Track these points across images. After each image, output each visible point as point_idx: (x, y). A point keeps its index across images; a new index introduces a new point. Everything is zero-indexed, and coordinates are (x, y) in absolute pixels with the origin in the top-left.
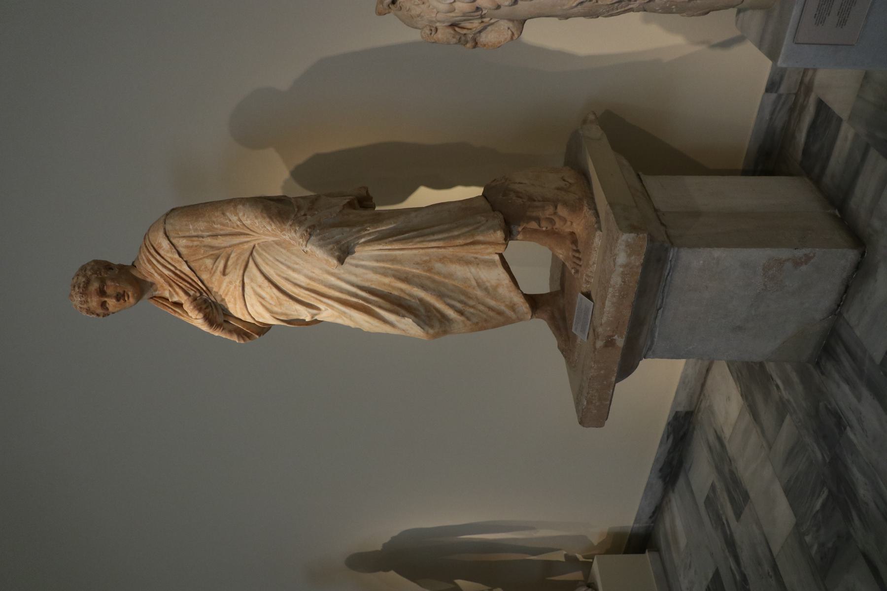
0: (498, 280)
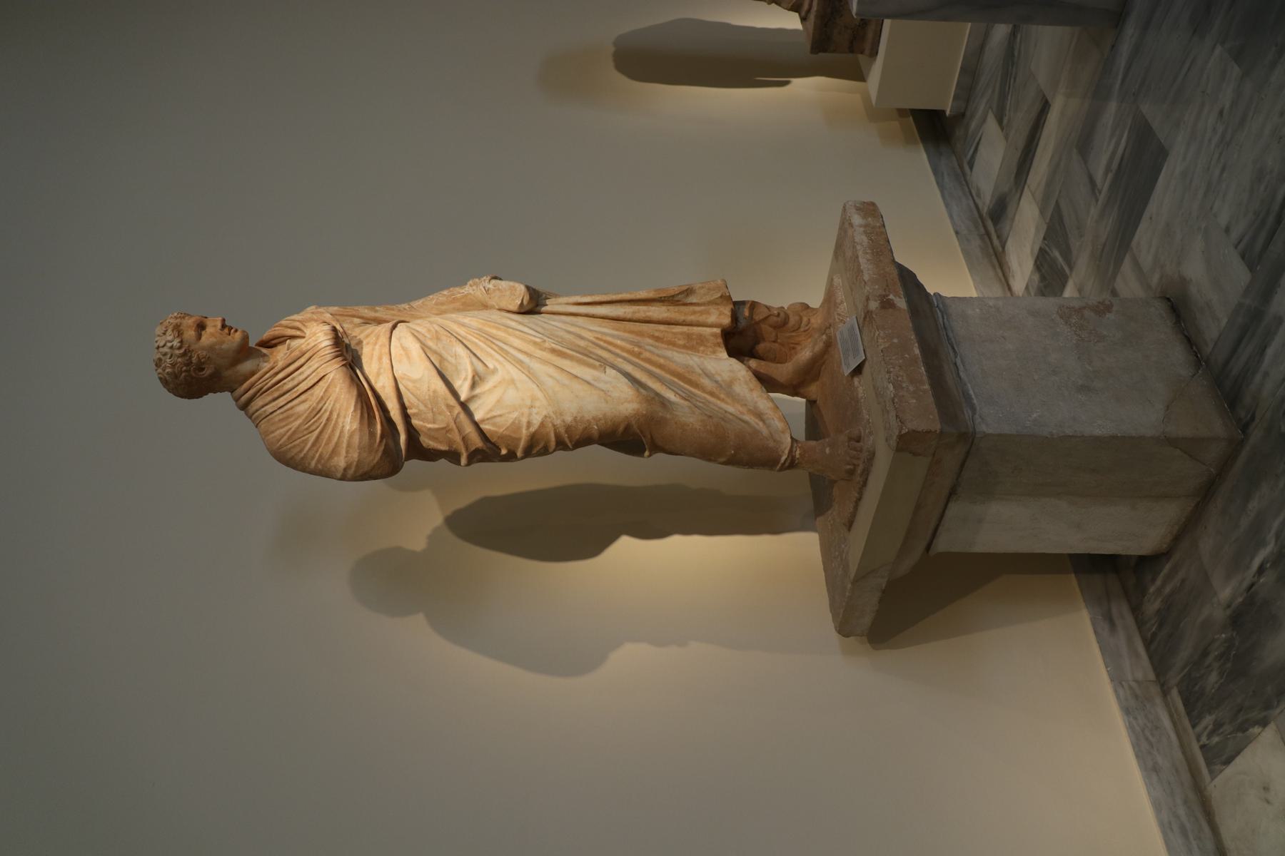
0: (731, 371)
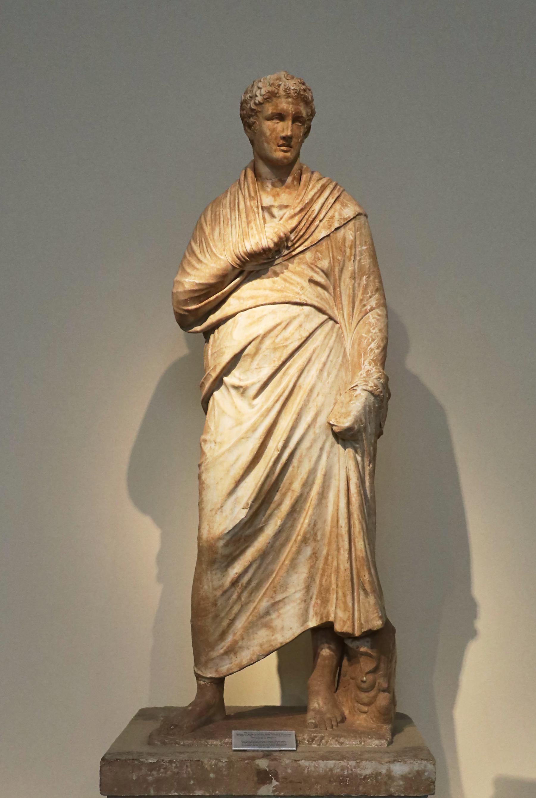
0: (283, 628)
